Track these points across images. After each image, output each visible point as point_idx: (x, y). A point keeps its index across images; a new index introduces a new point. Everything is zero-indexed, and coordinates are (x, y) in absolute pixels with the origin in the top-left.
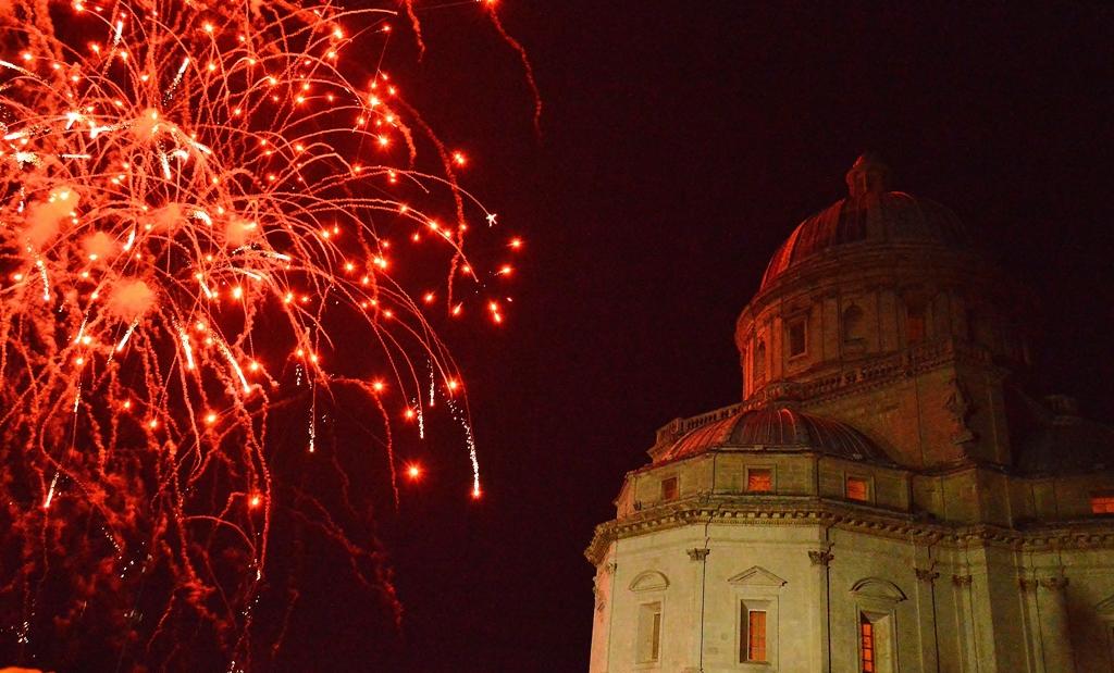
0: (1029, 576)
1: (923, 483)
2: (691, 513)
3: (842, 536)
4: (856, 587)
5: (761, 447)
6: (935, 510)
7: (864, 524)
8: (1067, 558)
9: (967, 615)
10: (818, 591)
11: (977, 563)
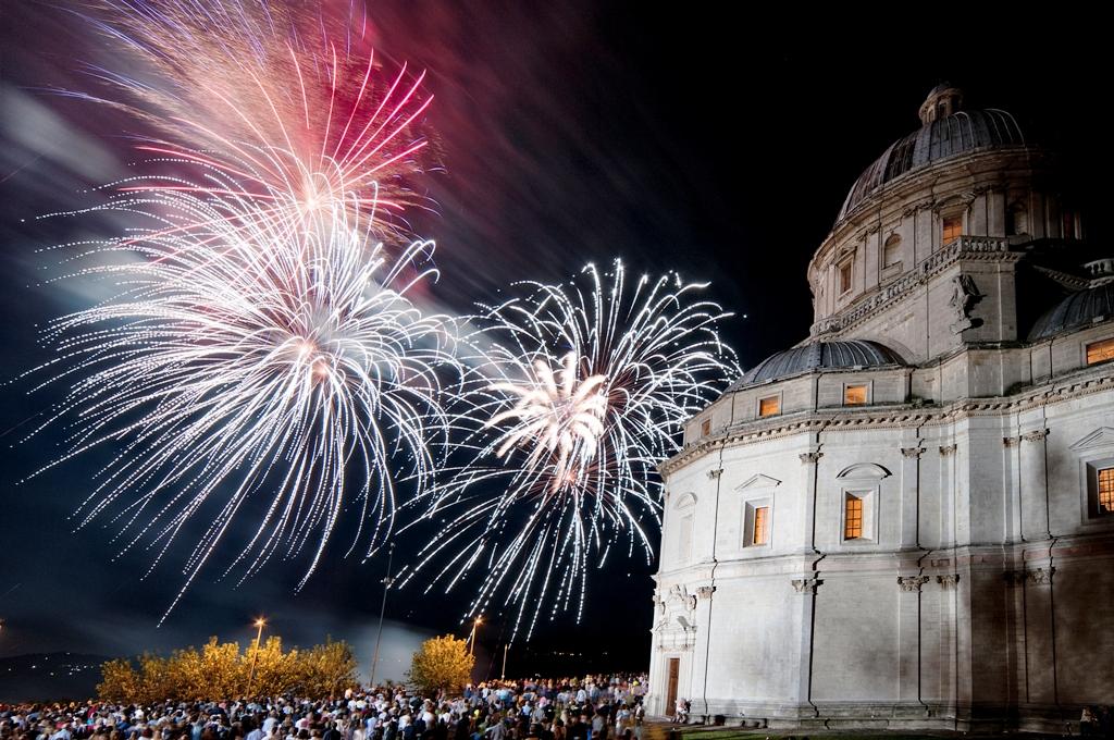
0: (1014, 434)
1: (919, 376)
2: (708, 444)
3: (831, 437)
4: (843, 474)
5: (770, 380)
6: (934, 397)
7: (853, 422)
8: (1051, 411)
9: (951, 479)
10: (806, 481)
11: (962, 433)
